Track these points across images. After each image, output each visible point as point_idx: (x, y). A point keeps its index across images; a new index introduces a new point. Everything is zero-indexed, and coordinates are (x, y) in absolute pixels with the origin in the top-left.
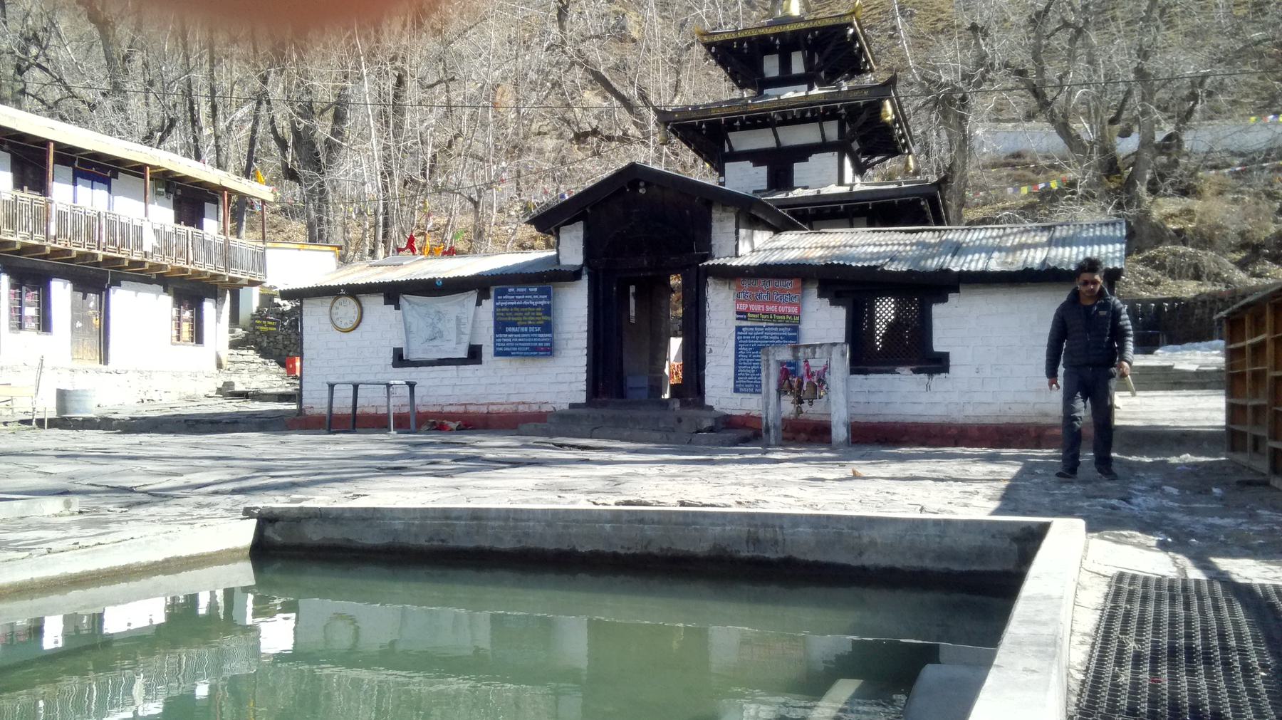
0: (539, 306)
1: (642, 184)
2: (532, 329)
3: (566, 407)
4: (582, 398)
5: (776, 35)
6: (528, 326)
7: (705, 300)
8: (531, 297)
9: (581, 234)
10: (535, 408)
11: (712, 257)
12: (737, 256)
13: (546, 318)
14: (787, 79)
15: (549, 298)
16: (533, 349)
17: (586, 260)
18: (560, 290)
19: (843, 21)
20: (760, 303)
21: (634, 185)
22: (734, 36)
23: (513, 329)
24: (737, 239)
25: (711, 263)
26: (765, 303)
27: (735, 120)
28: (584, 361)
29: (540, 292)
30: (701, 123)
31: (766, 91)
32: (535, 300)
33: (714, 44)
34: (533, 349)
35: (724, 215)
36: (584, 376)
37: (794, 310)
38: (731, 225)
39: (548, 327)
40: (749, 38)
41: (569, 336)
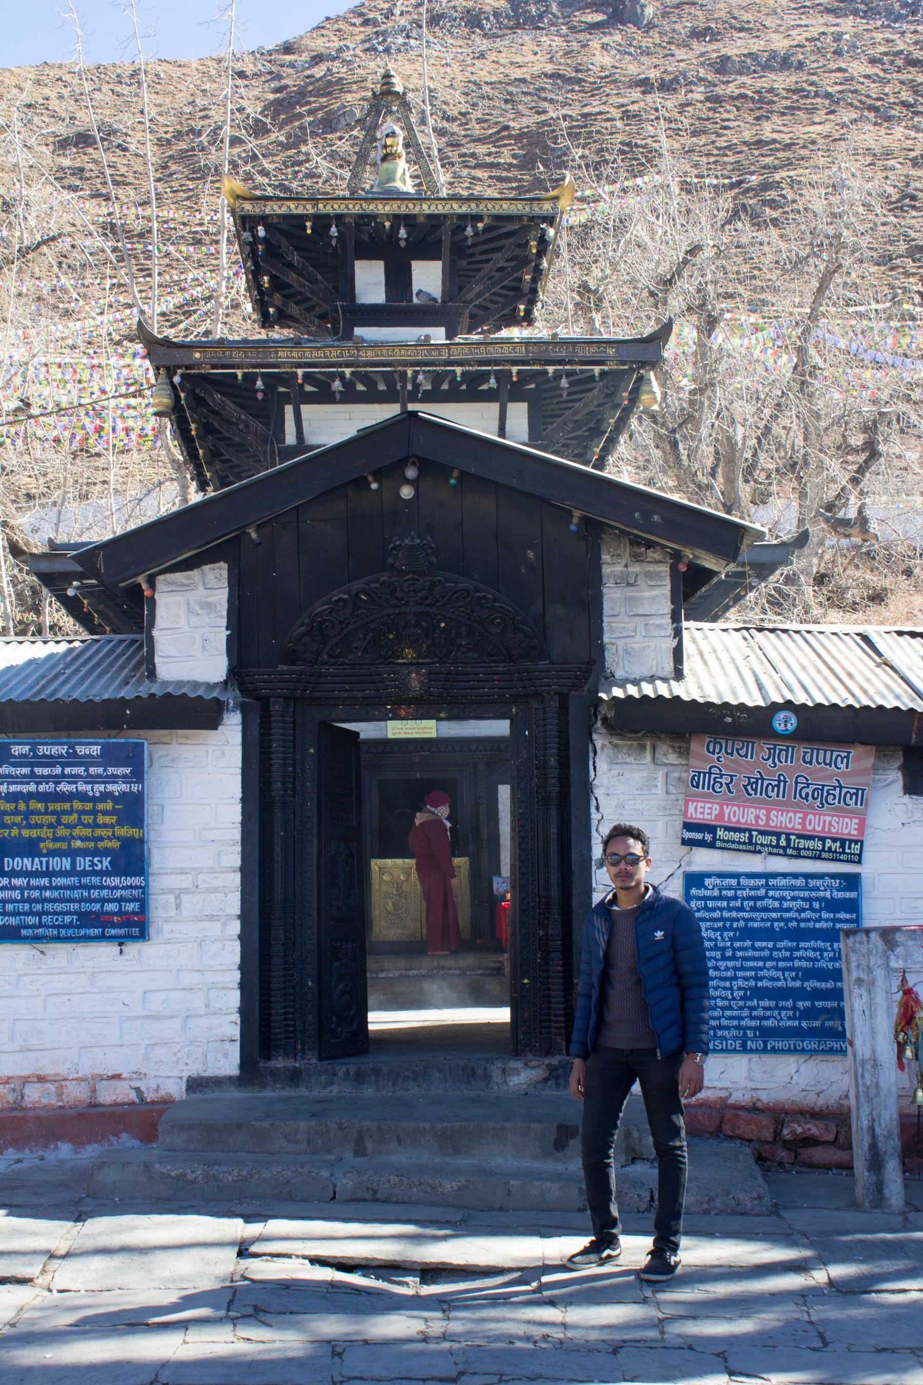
0: (105, 796)
1: (411, 473)
2: (83, 863)
3: (176, 1089)
4: (229, 1063)
5: (397, 219)
6: (72, 853)
7: (587, 788)
8: (83, 768)
9: (221, 597)
10: (76, 1093)
11: (611, 680)
12: (679, 675)
13: (124, 831)
14: (400, 308)
15: (138, 775)
16: (86, 919)
17: (233, 671)
18: (159, 751)
19: (537, 210)
20: (758, 804)
21: (390, 472)
22: (310, 209)
23: (27, 862)
24: (678, 633)
25: (617, 692)
26: (770, 805)
27: (333, 376)
28: (232, 953)
29: (110, 757)
30: (250, 379)
31: (358, 331)
32: (92, 780)
33: (263, 219)
34: (86, 919)
35: (635, 568)
36: (234, 998)
37: (846, 827)
38: (657, 596)
39: (132, 859)
40: (339, 217)
41: (184, 882)
